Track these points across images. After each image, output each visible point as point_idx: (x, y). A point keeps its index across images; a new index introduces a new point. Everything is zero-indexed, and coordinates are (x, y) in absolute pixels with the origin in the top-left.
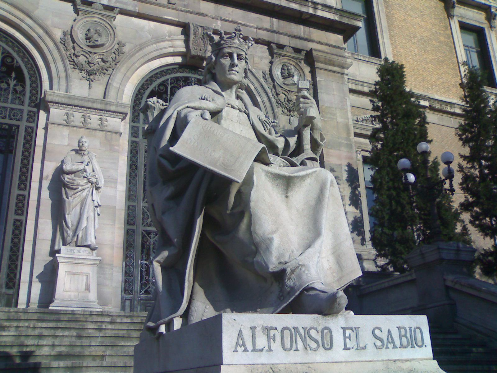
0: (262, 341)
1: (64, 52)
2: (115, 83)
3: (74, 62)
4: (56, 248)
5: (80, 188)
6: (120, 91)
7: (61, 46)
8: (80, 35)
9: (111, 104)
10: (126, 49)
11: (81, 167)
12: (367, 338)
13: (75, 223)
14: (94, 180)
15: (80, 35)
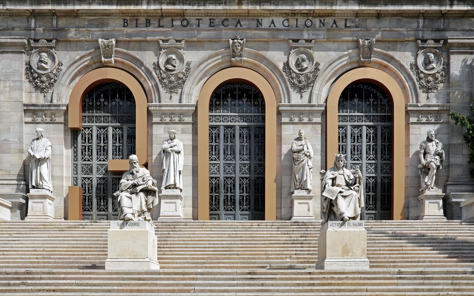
0: (334, 225)
1: (286, 77)
2: (315, 91)
3: (291, 82)
4: (292, 191)
5: (302, 159)
6: (319, 96)
7: (284, 74)
8: (292, 63)
9: (314, 106)
10: (320, 67)
11: (301, 147)
12: (352, 224)
13: (300, 178)
14: (308, 154)
15: (292, 63)
